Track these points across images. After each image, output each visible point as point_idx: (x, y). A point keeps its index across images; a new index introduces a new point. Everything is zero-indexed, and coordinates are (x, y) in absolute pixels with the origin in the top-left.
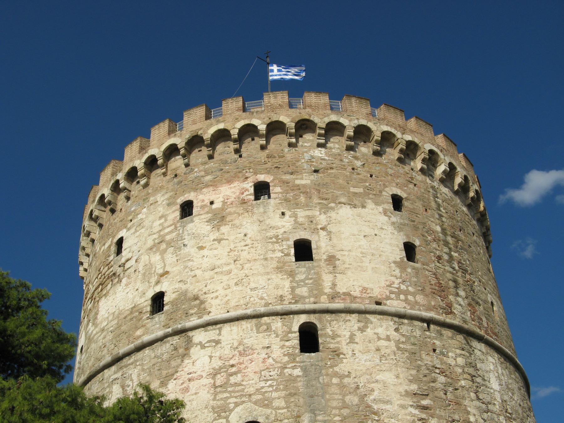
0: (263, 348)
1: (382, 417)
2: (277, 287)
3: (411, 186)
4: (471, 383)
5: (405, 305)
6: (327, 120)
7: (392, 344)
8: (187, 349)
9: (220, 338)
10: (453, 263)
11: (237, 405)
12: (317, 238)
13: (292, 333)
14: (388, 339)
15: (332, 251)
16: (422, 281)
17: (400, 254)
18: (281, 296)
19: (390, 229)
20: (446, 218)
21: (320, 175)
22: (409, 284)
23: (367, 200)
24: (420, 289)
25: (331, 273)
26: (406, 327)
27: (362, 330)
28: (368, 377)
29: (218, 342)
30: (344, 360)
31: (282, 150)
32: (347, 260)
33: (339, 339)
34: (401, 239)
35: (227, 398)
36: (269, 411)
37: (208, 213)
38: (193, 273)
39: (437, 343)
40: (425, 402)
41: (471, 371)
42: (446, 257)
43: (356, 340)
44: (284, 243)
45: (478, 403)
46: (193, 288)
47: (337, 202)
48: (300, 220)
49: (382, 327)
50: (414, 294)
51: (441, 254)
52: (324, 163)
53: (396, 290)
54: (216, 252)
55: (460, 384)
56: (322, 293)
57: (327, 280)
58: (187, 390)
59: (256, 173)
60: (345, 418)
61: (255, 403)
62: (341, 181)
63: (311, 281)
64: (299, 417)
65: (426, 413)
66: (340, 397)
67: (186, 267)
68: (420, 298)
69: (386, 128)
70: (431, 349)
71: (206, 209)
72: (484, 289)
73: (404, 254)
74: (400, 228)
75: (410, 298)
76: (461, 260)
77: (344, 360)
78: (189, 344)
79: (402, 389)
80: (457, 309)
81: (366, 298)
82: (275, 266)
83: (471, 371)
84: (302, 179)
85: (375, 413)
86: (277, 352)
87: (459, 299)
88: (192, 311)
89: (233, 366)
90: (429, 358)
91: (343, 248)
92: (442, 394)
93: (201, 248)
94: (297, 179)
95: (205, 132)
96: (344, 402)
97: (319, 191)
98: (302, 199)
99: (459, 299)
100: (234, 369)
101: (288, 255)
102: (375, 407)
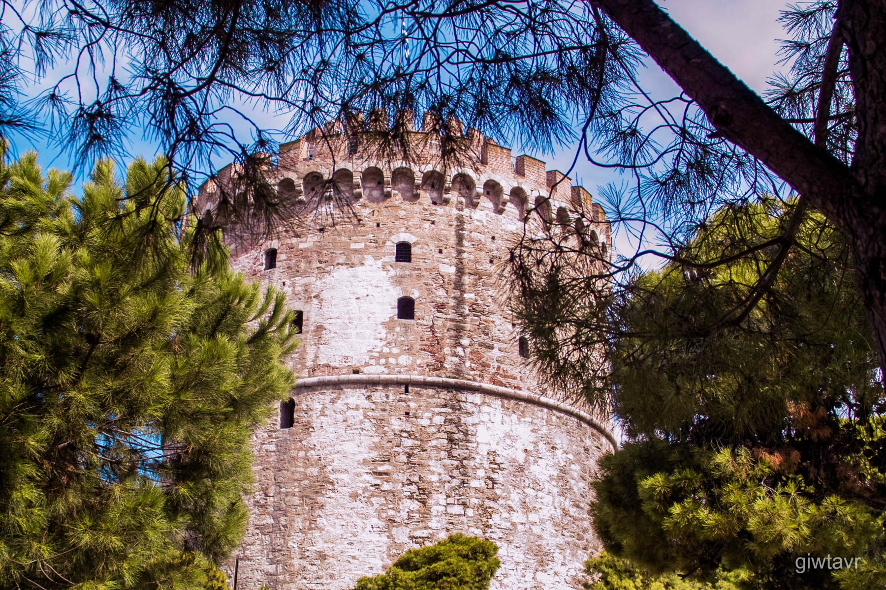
1: (336, 486)
3: (427, 225)
4: (446, 441)
5: (383, 369)
7: (359, 415)
12: (308, 309)
14: (357, 408)
15: (321, 321)
16: (411, 338)
19: (386, 284)
25: (315, 344)
26: (379, 395)
27: (333, 401)
30: (313, 434)
33: (310, 413)
34: (396, 294)
39: (413, 405)
40: (381, 469)
41: (449, 428)
42: (452, 303)
43: (327, 413)
45: (448, 462)
48: (299, 289)
49: (353, 396)
50: (396, 356)
53: (378, 355)
55: (430, 444)
56: (304, 366)
57: (311, 352)
60: (304, 489)
62: (343, 239)
64: (267, 489)
66: (302, 470)
68: (404, 360)
70: (403, 413)
73: (396, 311)
74: (398, 281)
75: (392, 360)
77: (313, 434)
79: (360, 458)
80: (450, 363)
81: (343, 368)
83: (449, 428)
85: (332, 483)
87: (459, 350)
90: (398, 422)
91: (332, 316)
92: (404, 458)
94: (301, 242)
96: (305, 474)
98: (303, 265)
99: (459, 350)
102: (332, 477)
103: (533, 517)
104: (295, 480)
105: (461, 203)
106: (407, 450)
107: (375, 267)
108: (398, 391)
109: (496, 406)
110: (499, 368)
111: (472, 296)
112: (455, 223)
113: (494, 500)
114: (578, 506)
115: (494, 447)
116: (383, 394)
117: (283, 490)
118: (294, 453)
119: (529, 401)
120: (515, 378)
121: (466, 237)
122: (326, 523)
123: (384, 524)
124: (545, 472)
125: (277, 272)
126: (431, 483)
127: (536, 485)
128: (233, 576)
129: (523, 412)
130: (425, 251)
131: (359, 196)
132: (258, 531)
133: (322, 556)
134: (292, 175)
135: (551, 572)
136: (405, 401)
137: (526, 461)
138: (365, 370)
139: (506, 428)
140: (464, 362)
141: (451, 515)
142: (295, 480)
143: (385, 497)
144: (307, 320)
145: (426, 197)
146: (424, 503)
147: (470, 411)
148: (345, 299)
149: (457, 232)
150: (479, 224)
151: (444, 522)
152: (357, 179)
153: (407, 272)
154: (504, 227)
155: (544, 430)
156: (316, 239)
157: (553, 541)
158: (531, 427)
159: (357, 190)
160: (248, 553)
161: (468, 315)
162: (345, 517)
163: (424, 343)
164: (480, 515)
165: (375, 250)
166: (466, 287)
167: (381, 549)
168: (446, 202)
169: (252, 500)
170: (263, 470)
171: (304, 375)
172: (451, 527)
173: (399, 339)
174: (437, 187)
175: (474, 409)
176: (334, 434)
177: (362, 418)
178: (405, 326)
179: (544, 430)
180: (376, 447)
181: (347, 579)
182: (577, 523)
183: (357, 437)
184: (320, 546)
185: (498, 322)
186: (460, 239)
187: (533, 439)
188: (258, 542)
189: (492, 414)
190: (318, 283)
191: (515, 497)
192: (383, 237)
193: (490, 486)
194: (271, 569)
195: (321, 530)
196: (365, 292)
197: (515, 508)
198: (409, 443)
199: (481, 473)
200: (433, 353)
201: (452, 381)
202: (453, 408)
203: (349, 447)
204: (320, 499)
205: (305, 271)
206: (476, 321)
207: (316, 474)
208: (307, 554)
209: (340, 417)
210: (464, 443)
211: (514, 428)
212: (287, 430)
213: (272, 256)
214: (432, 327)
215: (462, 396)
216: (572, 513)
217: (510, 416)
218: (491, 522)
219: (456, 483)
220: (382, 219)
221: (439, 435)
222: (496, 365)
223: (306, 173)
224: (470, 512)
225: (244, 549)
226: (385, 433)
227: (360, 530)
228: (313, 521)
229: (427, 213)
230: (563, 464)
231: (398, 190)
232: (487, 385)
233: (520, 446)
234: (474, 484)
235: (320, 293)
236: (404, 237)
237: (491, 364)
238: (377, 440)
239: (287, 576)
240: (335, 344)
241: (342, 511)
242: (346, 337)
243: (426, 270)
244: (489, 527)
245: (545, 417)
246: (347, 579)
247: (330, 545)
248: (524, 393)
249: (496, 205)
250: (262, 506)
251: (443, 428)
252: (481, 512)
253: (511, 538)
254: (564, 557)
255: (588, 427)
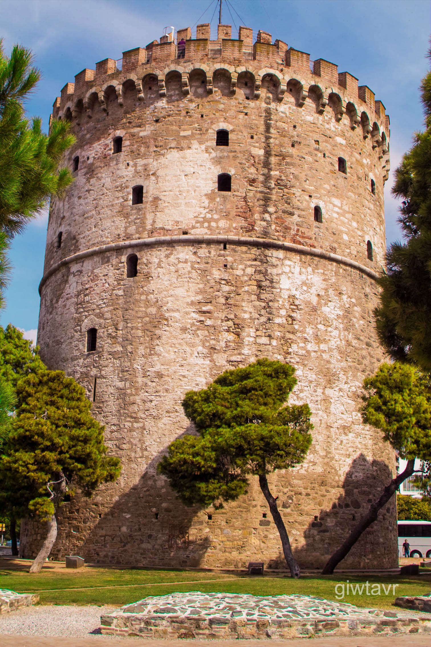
0: (104, 276)
1: (170, 322)
2: (117, 228)
3: (241, 116)
4: (256, 287)
5: (206, 231)
6: (167, 71)
7: (188, 267)
8: (68, 277)
9: (83, 269)
10: (270, 183)
11: (86, 317)
12: (148, 184)
13: (121, 263)
14: (186, 262)
15: (157, 193)
16: (228, 207)
17: (212, 185)
18: (119, 235)
19: (209, 164)
20: (274, 138)
21: (158, 124)
22: (214, 212)
23: (192, 141)
24: (225, 214)
25: (153, 212)
26: (203, 251)
27: (167, 256)
28: (165, 293)
29: (81, 272)
30: (152, 282)
31: (135, 105)
32: (167, 199)
33: (150, 265)
34: (217, 171)
35: (82, 312)
36: (102, 321)
37: (85, 167)
38: (73, 218)
39: (230, 259)
40: (204, 309)
42: (261, 178)
44: (125, 190)
45: (257, 303)
46: (74, 230)
47: (168, 148)
48: (139, 168)
49: (183, 252)
51: (256, 177)
52: (164, 113)
54: (86, 201)
55: (243, 290)
56: (144, 229)
57: (150, 218)
58: (65, 306)
59: (115, 130)
60: (146, 324)
61: (95, 316)
62: (174, 128)
63: (138, 221)
64: (117, 324)
65: (205, 316)
66: (144, 309)
67: (72, 213)
68: (223, 223)
69: (218, 66)
70: (222, 265)
71: (85, 165)
72: (307, 198)
74: (218, 161)
75: (213, 224)
76: (281, 177)
77: (152, 282)
78: (69, 273)
79: (189, 300)
81: (175, 230)
82: (117, 210)
84: (145, 130)
85: (167, 320)
86: (111, 280)
88: (72, 248)
89: (87, 289)
91: (166, 189)
92: (223, 301)
93: (80, 198)
94: (141, 131)
95: (84, 97)
96: (146, 313)
97: (155, 140)
98: (143, 149)
99: (267, 216)
100: (87, 292)
101: (126, 200)
102: (167, 315)
103: (323, 346)
104: (138, 318)
105: (269, 98)
106: (225, 294)
107: (199, 150)
108: (218, 248)
109: (296, 260)
110: (298, 230)
111: (277, 173)
112: (264, 114)
113: (293, 333)
114: (358, 339)
115: (294, 292)
116: (207, 250)
117: (129, 325)
118: (137, 297)
119: (322, 256)
120: (311, 239)
121: (272, 125)
122: (162, 350)
123: (207, 351)
124: (333, 312)
125: (122, 154)
126: (244, 319)
127: (327, 323)
128: (93, 390)
129: (316, 265)
130: (240, 137)
131: (186, 93)
132: (110, 356)
133: (160, 375)
134: (133, 77)
135: (337, 389)
136: (223, 256)
137: (319, 303)
138: (192, 231)
139: (304, 277)
140: (270, 226)
141: (260, 344)
142: (138, 318)
143: (208, 330)
144: (147, 192)
145: (241, 93)
146: (238, 335)
147: (275, 264)
148: (176, 176)
149: (266, 121)
150: (283, 115)
151: (254, 349)
152: (185, 79)
153: (226, 154)
154: (303, 118)
155: (333, 280)
156: (152, 128)
157: (339, 365)
158: (323, 277)
159: (185, 88)
160: (103, 373)
161: (274, 188)
162: (177, 346)
163: (239, 210)
164: (282, 344)
165: (199, 136)
166: (273, 166)
167: (205, 370)
168: (257, 97)
169: (106, 333)
170: (114, 309)
171: (144, 236)
172: (259, 353)
173: (219, 208)
174: (248, 85)
175: (278, 263)
176: (168, 282)
177: (190, 269)
178: (224, 197)
179: (333, 280)
180: (201, 292)
181: (179, 392)
182: (357, 351)
183: (186, 284)
184: (158, 367)
185: (297, 194)
186: (268, 127)
187: (324, 286)
188: (111, 365)
189: (292, 267)
190: (155, 163)
191: (310, 330)
192: (206, 126)
193: (290, 322)
194: (121, 385)
195: (159, 355)
196: (192, 170)
197: (309, 339)
198: (226, 288)
199: (283, 312)
200: (246, 218)
201: (261, 240)
202: (261, 261)
203: (180, 292)
204: (158, 332)
205: (145, 154)
206: (280, 193)
207: (154, 312)
208: (148, 373)
209: (173, 269)
210: (270, 289)
211: (309, 277)
212: (132, 279)
213: (118, 142)
214: (245, 198)
215: (269, 252)
216: (354, 344)
217: (306, 268)
218: (290, 350)
219: (263, 319)
220: (205, 111)
221: (250, 283)
222: (296, 228)
223: (143, 75)
224: (274, 343)
225: (101, 370)
226: (208, 281)
227: (188, 355)
228: (152, 349)
229: (241, 106)
230: (347, 306)
231: (218, 87)
232: (288, 244)
233: (313, 291)
234: (278, 320)
235: (156, 171)
236: (223, 126)
237: (292, 227)
238: (201, 286)
239: (133, 390)
240: (169, 212)
241: (174, 341)
242: (177, 205)
243: (240, 152)
244: (289, 353)
245: (334, 269)
246: (179, 392)
247: (166, 367)
248: (318, 250)
249: (297, 100)
250: (113, 337)
251: (253, 277)
252: (282, 342)
253: (306, 362)
254: (347, 378)
255: (368, 278)
